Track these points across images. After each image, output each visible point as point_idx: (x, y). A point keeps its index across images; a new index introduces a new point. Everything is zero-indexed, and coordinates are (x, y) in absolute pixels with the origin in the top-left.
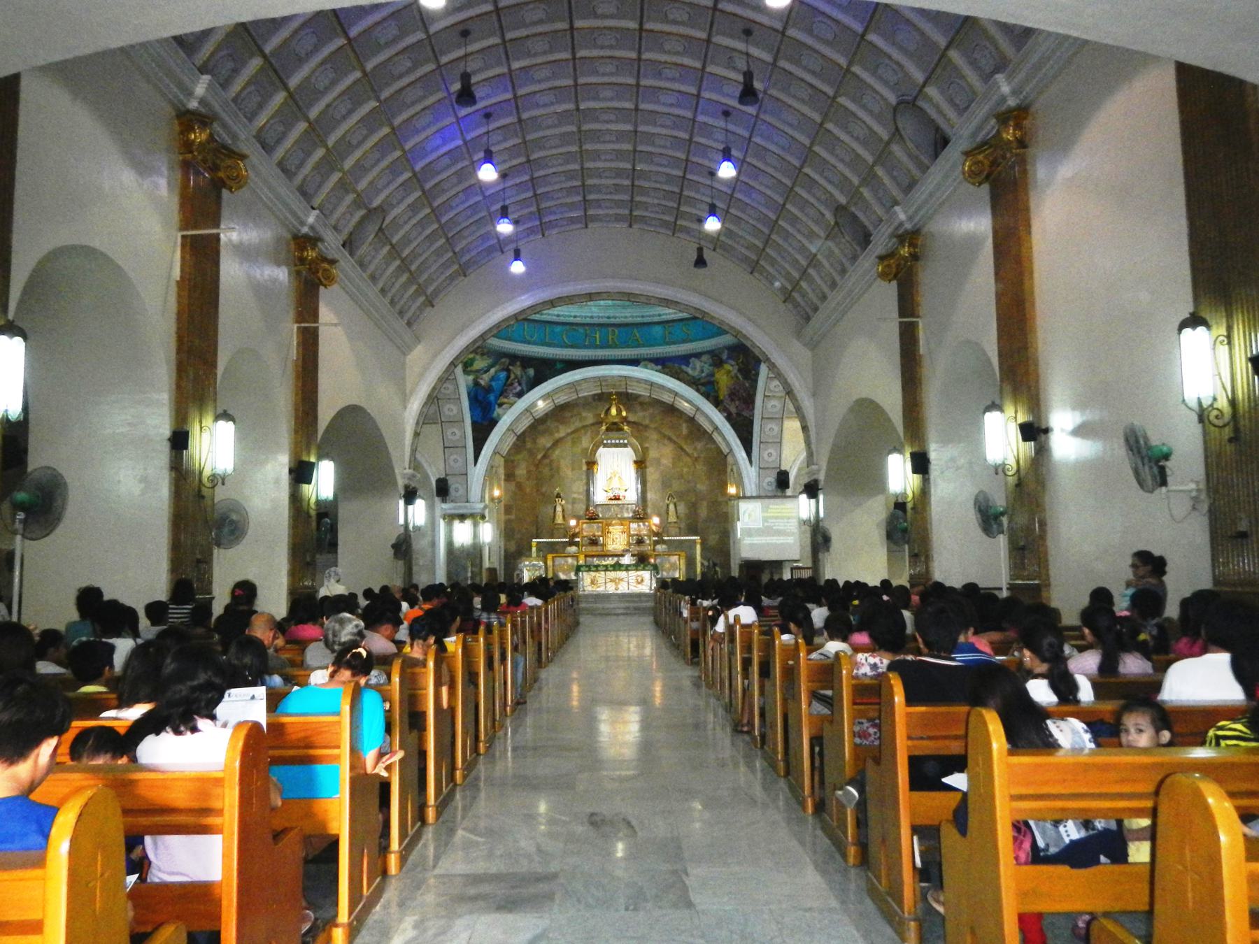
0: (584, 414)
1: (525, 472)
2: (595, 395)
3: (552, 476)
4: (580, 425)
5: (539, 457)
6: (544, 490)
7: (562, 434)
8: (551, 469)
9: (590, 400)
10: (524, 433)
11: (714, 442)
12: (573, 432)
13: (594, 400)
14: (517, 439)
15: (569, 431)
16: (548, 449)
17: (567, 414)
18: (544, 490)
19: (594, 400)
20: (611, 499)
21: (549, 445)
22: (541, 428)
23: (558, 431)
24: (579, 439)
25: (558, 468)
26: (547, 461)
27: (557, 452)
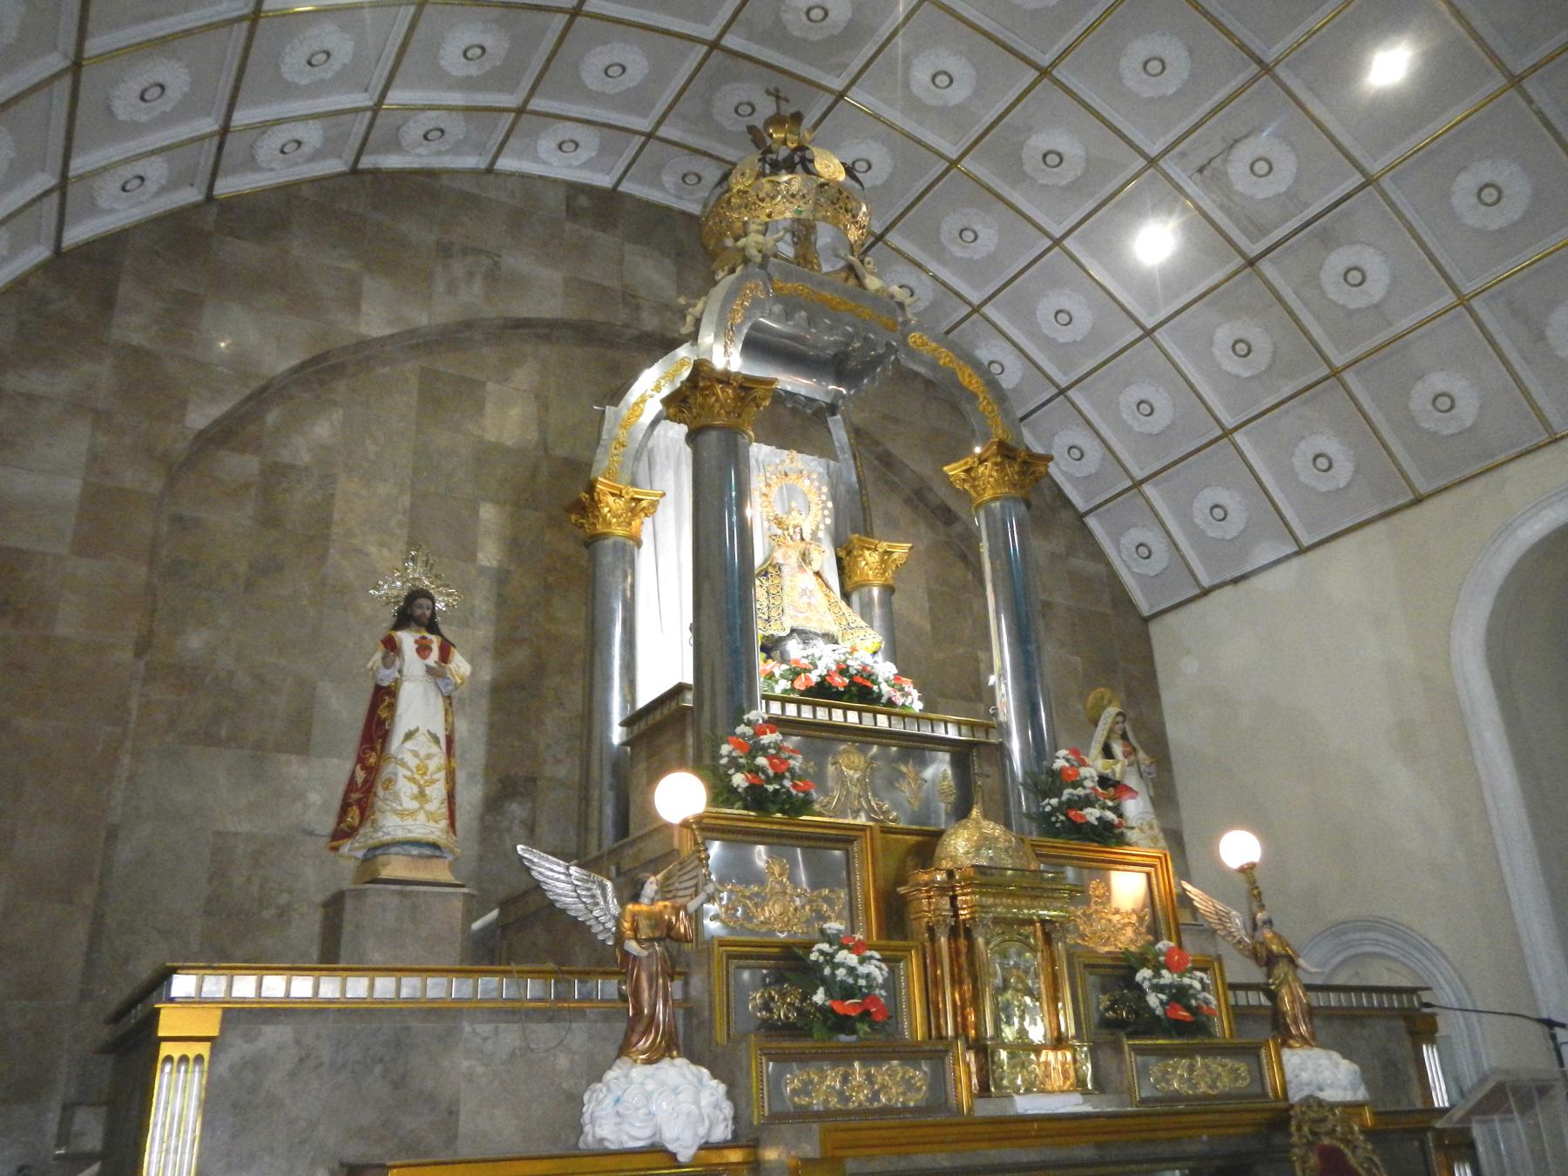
0: (517, 261)
1: (72, 488)
2: (575, 189)
3: (268, 568)
4: (490, 312)
5: (200, 417)
6: (195, 641)
7: (374, 322)
8: (270, 519)
9: (554, 201)
10: (115, 241)
11: (1099, 554)
12: (453, 337)
13: (573, 213)
14: (44, 267)
15: (421, 318)
16: (264, 395)
17: (416, 230)
18: (195, 641)
19: (573, 213)
20: (822, 692)
21: (279, 362)
22: (245, 252)
23: (353, 303)
24: (469, 391)
25: (320, 526)
26: (241, 465)
27: (324, 429)
